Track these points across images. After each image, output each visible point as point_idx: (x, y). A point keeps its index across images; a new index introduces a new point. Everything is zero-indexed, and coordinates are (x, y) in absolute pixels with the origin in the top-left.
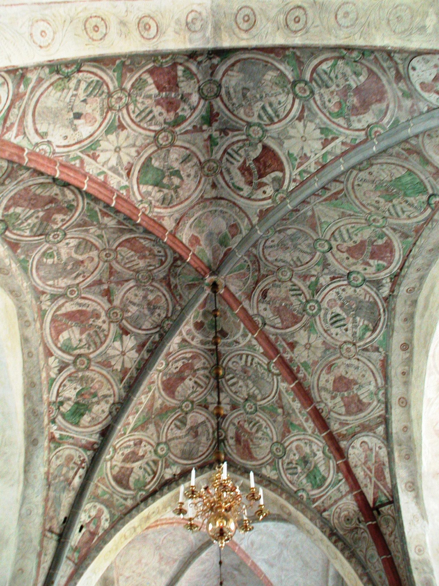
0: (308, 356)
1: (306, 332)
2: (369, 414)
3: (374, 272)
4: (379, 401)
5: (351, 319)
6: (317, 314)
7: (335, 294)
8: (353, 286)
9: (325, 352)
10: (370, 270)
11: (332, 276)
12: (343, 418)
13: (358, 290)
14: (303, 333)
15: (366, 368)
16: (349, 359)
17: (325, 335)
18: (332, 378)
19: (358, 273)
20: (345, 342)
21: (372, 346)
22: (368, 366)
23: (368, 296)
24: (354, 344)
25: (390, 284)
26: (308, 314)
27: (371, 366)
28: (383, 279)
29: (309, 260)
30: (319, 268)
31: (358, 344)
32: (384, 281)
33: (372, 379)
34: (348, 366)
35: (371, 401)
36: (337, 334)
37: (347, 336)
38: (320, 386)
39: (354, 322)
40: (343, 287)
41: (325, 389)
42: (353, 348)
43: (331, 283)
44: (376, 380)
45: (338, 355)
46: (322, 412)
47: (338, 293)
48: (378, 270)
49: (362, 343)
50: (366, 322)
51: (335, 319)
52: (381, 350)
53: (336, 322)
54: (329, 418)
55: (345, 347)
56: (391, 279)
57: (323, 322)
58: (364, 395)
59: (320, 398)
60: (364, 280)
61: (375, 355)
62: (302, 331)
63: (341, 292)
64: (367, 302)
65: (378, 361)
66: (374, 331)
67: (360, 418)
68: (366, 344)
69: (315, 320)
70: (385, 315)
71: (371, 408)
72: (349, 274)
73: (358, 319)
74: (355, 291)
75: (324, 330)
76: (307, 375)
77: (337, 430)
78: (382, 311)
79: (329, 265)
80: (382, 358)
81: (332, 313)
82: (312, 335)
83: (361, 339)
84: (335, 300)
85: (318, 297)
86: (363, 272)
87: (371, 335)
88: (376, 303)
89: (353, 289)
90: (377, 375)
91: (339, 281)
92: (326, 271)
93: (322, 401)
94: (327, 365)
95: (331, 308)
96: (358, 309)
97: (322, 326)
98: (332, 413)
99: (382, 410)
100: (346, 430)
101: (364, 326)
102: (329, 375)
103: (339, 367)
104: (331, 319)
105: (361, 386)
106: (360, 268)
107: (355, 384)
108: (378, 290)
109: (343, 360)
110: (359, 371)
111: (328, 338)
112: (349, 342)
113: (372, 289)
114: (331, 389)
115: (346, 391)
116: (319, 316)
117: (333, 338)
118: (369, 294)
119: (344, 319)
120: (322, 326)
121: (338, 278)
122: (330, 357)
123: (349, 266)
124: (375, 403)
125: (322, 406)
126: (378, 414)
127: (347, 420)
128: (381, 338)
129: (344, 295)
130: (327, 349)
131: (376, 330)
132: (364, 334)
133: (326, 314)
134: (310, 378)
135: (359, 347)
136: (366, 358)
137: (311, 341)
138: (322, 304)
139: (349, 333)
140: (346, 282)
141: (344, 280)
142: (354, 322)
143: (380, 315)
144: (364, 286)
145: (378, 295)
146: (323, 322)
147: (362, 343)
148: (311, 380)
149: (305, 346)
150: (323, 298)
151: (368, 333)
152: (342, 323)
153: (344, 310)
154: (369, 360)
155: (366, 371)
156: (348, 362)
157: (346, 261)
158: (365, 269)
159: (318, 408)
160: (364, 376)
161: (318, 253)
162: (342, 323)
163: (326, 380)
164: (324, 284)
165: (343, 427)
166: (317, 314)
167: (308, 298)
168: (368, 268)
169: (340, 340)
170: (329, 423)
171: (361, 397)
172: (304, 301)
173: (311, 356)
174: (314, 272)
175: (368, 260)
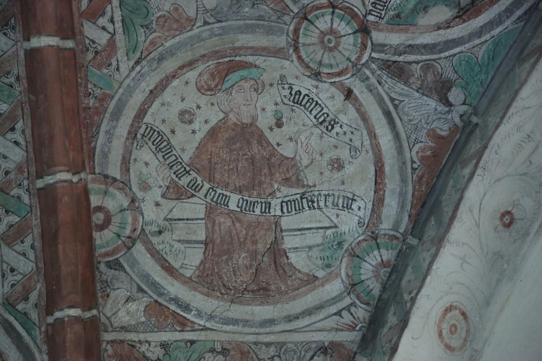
2: (289, 319)
4: (353, 286)
12: (174, 288)
15: (361, 139)
16: (317, 75)
18: (210, 115)
21: (427, 67)
22: (372, 135)
24: (364, 30)
27: (386, 140)
31: (377, 36)
33: (365, 190)
34: (297, 99)
35: (320, 274)
38: (148, 119)
41: (162, 145)
42: (349, 43)
44: (379, 202)
45: (282, 41)
46: (102, 227)
49: (395, 39)
52: (455, 95)
54: (116, 265)
55: (324, 23)
58: (303, 238)
59: (126, 164)
61: (421, 108)
65: (423, 135)
67: (246, 323)
68: (412, 49)
71: (310, 299)
76: (121, 53)
77: (124, 329)
80: (443, 129)
87: (448, 25)
90: (392, 184)
93: (125, 185)
94: (216, 54)
98: (139, 249)
99: (352, 328)
100: (164, 345)
102: (203, 100)
105: (308, 200)
107: (287, 181)
109: (291, 68)
110: (329, 140)
114: (186, 158)
115: (239, 190)
122: (250, 29)
124: (335, 287)
125: (115, 201)
126: (326, 338)
127: (187, 308)
128: (481, 53)
131: (478, 13)
134: (124, 68)
135: (380, 47)
136: (380, 101)
147: (395, 39)
148: (126, 81)
154: (387, 114)
155: (354, 150)
156: (305, 85)
159: (95, 201)
160: (337, 165)
163: (188, 111)
165: (160, 329)
170: (107, 284)
171: (289, 242)
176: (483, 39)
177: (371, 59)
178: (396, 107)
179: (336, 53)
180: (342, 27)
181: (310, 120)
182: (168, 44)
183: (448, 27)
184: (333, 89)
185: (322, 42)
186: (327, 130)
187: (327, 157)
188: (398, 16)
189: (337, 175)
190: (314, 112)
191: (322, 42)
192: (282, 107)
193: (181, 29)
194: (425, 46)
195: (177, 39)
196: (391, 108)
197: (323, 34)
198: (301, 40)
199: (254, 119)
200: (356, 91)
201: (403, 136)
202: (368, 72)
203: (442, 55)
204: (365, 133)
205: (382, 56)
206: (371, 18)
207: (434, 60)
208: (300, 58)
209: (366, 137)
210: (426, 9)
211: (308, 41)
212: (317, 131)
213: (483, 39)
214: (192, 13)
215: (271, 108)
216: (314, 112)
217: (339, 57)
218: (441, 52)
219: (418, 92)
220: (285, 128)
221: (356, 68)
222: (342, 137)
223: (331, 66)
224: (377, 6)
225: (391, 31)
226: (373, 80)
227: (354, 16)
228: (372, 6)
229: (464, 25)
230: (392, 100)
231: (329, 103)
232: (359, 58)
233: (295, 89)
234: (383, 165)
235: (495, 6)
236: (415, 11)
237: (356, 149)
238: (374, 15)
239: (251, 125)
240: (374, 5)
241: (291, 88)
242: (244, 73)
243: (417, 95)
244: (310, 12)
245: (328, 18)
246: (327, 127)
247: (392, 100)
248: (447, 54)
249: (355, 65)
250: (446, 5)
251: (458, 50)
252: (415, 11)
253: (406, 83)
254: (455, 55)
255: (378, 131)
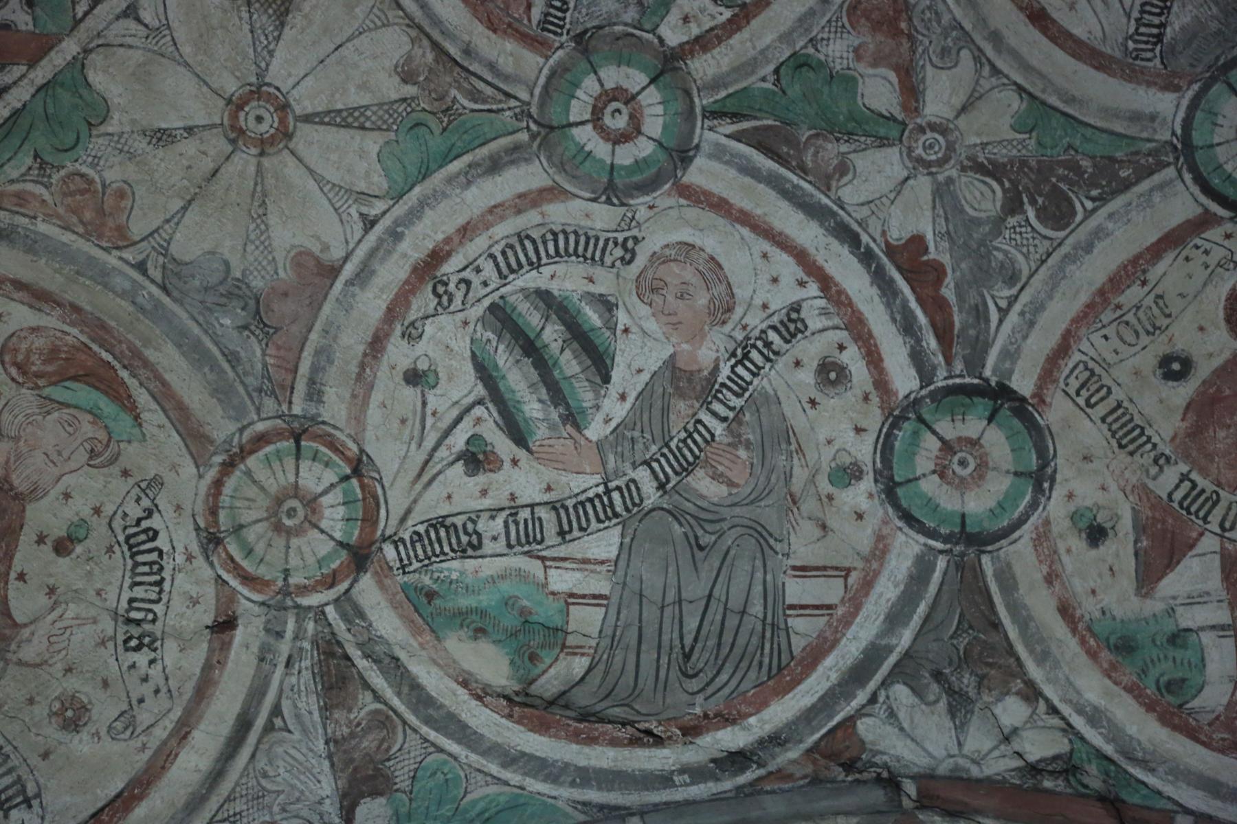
0: (162, 137)
1: (392, 89)
3: (1088, 608)
5: (586, 482)
6: (573, 163)
7: (780, 300)
8: (886, 447)
9: (231, 290)
10: (1105, 581)
11: (937, 252)
13: (862, 494)
14: (376, 67)
15: (159, 718)
16: (212, 540)
17: (393, 272)
19: (1040, 479)
20: (359, 466)
21: (384, 721)
22: (182, 732)
23: (830, 591)
24: (360, 557)
25: (999, 765)
26: (559, 83)
27: (192, 763)
28: (1032, 694)
29: (1082, 25)
30: (995, 125)
31: (367, 589)
32: (1012, 711)
34: (139, 542)
36: (414, 377)
37: (425, 475)
39: (573, 516)
40: (852, 358)
42: (315, 550)
43: (867, 257)
47: (792, 324)
48: (1118, 648)
49: (387, 623)
50: (587, 620)
51: (552, 335)
53: (530, 348)
56: (1067, 767)
57: (503, 230)
60: (971, 539)
62: (394, 43)
63: (811, 349)
64: (773, 596)
66: (525, 704)
68: (393, 667)
69: (515, 155)
70: (697, 774)
72: (1000, 396)
73: (604, 543)
74: (849, 474)
75: (437, 257)
78: (731, 738)
79: (1058, 214)
81: (607, 305)
82: (373, 143)
83: (425, 607)
84: (723, 309)
85: (719, 154)
86: (1056, 507)
87: (482, 694)
88: (784, 673)
89: (864, 451)
91: (908, 327)
92: (982, 198)
94: (99, 329)
95: (649, 288)
96: (699, 532)
97: (466, 232)
101: (547, 611)
103: (100, 455)
104: (544, 297)
106: (1092, 478)
108: (905, 671)
109: (187, 483)
110: (109, 662)
111: (372, 304)
112: (369, 508)
113: (895, 619)
116: (552, 193)
117: (377, 344)
118: (855, 603)
119: (574, 419)
120: (466, 232)
121: (936, 307)
122: (196, 354)
123: (1093, 387)
128: (481, 792)
129: (788, 380)
130: (259, 320)
131: (542, 727)
132: (478, 626)
133: (581, 246)
135: (352, 611)
136: (256, 693)
137: (308, 138)
138: (663, 198)
139: (459, 492)
140: (905, 381)
141: (918, 358)
142: (573, 516)
143: (691, 731)
144: (906, 548)
145: (858, 674)
146: (503, 230)
147: (387, 623)
149: (258, 91)
150: (720, 206)
151: (492, 665)
152: (533, 407)
153: (651, 403)
154: (244, 724)
155: (127, 721)
156: (177, 535)
157: (1148, 360)
158: (1096, 534)
160: (73, 716)
161: (1167, 105)
162: (533, 407)
164: (852, 193)
166: (573, 163)
167: (703, 67)
168: (1121, 550)
169: (374, 414)
172: (673, 34)
173: (169, 166)
174: (941, 94)
175: (1209, 543)
176: (506, 775)
177: (320, 612)
178: (269, 728)
179: (280, 542)
180: (334, 515)
181: (118, 593)
182: (42, 227)
183: (479, 698)
184: (210, 591)
185: (279, 502)
186: (126, 642)
187: (72, 684)
188: (431, 595)
189: (52, 732)
190: (139, 592)
191: (279, 502)
192: (99, 529)
193: (92, 232)
194: (416, 686)
195: (67, 237)
196: (260, 722)
197: (295, 491)
198: (251, 461)
199: (35, 493)
200: (239, 634)
201: (225, 787)
202: (291, 626)
203: (425, 730)
204: (177, 713)
205: (340, 627)
206: (389, 551)
207: (405, 722)
208: (218, 484)
209: (169, 724)
210: (479, 632)
211: (262, 475)
212: (107, 625)
213: (506, 775)
214: (138, 228)
215: (80, 507)
216: (139, 592)
217: (276, 555)
218: (428, 721)
219: (327, 743)
220: (64, 562)
221: (282, 599)
222: (133, 680)
223: (249, 552)
224: (418, 545)
225: (395, 606)
226: (285, 648)
227: (370, 519)
228: (411, 537)
229: (504, 721)
230: (277, 711)
231: (178, 604)
232: (304, 590)
233: (155, 522)
234: (140, 798)
235: (575, 747)
236: (461, 617)
237: (131, 724)
238: (399, 554)
239: (19, 497)
240: (416, 538)
241: (149, 514)
242: (107, 407)
243: (320, 745)
244: (316, 437)
245: (330, 477)
246: (130, 638)
247: (277, 711)
248: (433, 735)
249: (285, 592)
250: (512, 662)
251: (453, 747)
252: (461, 617)
253: (326, 709)
254: (441, 750)
255: (198, 736)
